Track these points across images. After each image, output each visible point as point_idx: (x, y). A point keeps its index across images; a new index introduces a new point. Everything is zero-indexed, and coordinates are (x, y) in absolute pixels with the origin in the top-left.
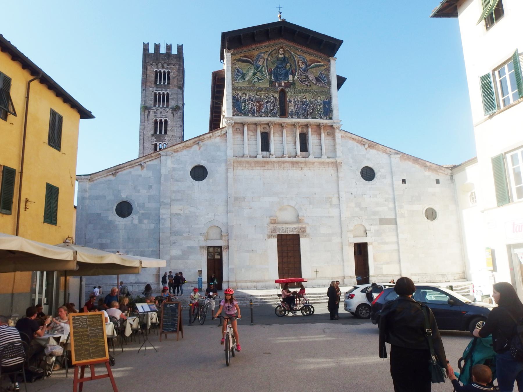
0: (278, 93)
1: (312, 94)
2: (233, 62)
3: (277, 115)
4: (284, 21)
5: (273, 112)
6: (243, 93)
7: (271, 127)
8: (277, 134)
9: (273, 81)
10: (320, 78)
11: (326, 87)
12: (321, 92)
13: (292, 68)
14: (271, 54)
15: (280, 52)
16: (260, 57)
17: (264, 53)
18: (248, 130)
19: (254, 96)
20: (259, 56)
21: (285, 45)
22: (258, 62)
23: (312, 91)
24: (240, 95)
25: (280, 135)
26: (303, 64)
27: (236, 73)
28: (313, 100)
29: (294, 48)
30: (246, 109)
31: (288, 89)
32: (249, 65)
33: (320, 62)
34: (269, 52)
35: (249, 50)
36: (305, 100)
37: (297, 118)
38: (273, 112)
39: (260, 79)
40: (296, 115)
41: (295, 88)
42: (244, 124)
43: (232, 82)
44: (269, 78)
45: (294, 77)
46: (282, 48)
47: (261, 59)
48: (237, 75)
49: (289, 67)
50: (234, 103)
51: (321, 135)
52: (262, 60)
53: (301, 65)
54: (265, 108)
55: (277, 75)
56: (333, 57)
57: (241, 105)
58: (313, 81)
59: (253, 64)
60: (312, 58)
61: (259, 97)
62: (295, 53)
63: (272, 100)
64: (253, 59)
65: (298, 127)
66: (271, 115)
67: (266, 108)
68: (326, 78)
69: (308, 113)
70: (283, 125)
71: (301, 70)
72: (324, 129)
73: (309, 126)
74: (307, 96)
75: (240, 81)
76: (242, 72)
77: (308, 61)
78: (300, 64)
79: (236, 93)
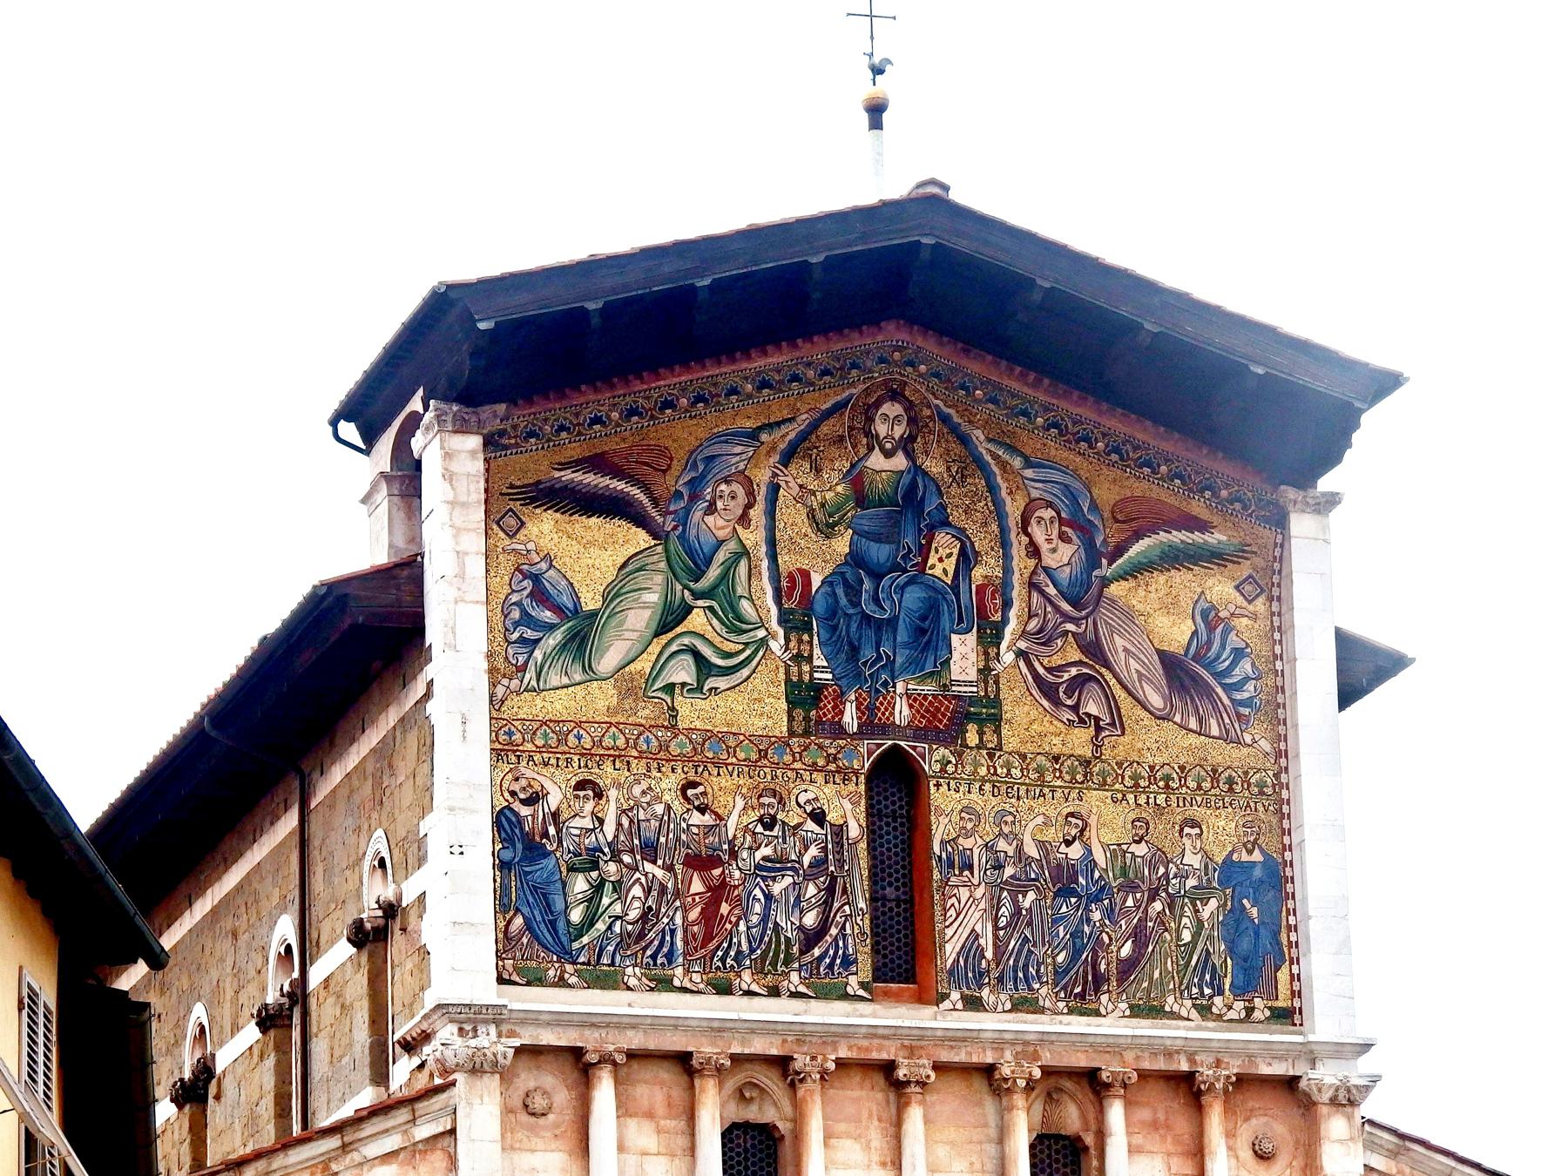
0: (862, 787)
1: (1131, 797)
2: (502, 505)
3: (853, 980)
4: (934, 197)
6: (581, 785)
7: (812, 1092)
8: (847, 1143)
10: (1197, 658)
11: (1248, 738)
12: (1206, 785)
13: (978, 573)
14: (807, 444)
15: (881, 429)
16: (718, 470)
18: (624, 1108)
19: (669, 808)
20: (712, 458)
21: (923, 368)
22: (697, 515)
23: (1136, 777)
24: (554, 800)
25: (876, 1158)
26: (1063, 538)
27: (519, 604)
28: (1140, 850)
29: (994, 401)
30: (601, 926)
31: (936, 757)
33: (1204, 527)
34: (791, 432)
35: (633, 412)
36: (1075, 852)
37: (1015, 1008)
38: (817, 952)
39: (720, 662)
41: (999, 747)
42: (592, 1058)
43: (493, 684)
44: (787, 656)
46: (895, 395)
47: (723, 487)
48: (527, 620)
49: (950, 565)
50: (503, 866)
51: (1203, 1156)
52: (730, 497)
53: (1044, 547)
54: (755, 919)
55: (854, 626)
56: (1311, 492)
57: (559, 885)
59: (655, 536)
60: (1139, 488)
61: (708, 819)
62: (1001, 444)
63: (813, 851)
65: (1019, 1100)
66: (803, 980)
67: (765, 918)
68: (1246, 667)
69: (1103, 967)
70: (901, 1073)
71: (1051, 590)
72: (1228, 1111)
73: (1108, 1086)
74: (1093, 821)
75: (555, 679)
76: (566, 601)
77: (1107, 515)
78: (1038, 533)
79: (523, 782)
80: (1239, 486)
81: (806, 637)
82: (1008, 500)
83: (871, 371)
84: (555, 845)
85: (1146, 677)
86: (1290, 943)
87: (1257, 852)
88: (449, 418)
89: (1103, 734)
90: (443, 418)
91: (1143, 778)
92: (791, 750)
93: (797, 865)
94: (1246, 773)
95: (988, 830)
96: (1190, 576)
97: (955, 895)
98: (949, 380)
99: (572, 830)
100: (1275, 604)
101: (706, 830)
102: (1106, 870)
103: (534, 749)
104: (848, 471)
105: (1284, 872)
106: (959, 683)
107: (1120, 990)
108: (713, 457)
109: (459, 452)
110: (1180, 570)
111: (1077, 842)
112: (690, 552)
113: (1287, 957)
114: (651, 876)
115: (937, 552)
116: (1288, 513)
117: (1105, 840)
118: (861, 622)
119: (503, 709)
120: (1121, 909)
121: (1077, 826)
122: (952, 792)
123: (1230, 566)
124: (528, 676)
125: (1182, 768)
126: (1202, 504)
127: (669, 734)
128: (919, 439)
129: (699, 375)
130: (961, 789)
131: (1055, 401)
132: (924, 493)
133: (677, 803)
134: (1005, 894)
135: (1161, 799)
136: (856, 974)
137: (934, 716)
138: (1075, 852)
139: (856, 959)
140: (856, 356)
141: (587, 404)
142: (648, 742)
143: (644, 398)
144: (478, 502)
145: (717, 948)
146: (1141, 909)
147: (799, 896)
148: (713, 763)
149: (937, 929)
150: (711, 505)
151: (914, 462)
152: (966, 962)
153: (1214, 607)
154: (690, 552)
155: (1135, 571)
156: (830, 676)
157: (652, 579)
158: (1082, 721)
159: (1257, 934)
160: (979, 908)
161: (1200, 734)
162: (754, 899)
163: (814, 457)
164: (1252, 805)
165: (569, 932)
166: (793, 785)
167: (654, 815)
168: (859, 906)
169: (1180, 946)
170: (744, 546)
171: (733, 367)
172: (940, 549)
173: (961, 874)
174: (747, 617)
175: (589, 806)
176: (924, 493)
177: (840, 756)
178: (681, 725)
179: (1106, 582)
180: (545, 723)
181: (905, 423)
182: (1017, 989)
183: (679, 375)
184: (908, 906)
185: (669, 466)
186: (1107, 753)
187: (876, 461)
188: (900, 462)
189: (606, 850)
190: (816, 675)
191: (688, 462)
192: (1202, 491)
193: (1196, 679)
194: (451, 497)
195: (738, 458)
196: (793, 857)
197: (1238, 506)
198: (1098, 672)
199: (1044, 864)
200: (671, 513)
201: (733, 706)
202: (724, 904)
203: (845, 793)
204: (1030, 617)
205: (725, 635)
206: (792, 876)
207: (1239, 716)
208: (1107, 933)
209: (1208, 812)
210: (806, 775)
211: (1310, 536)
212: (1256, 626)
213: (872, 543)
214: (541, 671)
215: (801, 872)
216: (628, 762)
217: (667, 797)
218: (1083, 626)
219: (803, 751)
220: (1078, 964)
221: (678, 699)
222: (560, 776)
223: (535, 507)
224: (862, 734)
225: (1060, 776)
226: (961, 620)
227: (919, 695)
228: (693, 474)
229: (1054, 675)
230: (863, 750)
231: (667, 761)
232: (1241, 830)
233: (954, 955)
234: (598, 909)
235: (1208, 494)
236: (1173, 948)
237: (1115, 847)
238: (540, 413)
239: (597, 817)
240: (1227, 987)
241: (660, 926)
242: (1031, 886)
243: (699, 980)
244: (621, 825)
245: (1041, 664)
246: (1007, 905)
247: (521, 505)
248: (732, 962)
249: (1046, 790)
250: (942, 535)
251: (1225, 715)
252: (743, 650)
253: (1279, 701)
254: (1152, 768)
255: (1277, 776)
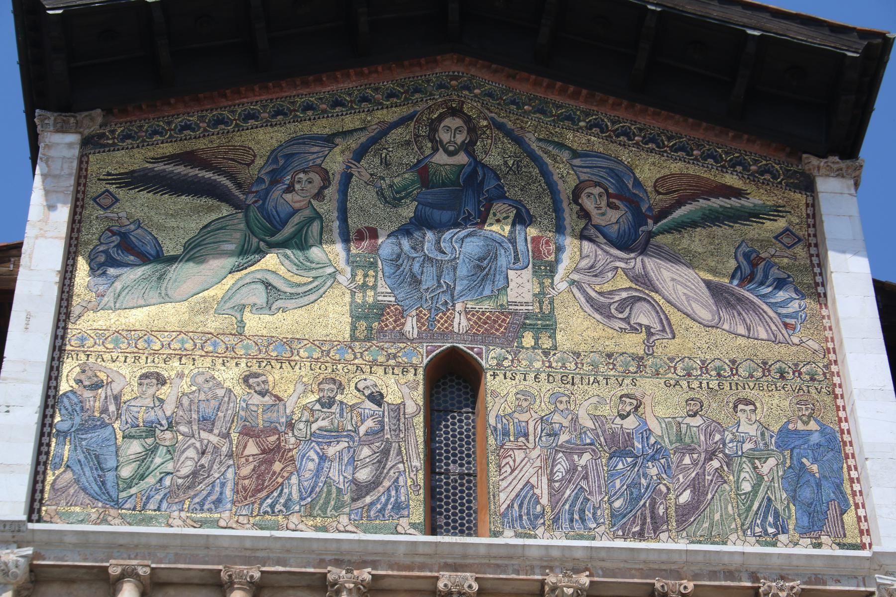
0: (420, 377)
1: (684, 384)
3: (404, 522)
5: (372, 504)
9: (389, 306)
11: (796, 340)
14: (377, 146)
15: (444, 137)
17: (329, 140)
20: (289, 157)
21: (477, 91)
26: (611, 206)
27: (105, 252)
28: (697, 421)
29: (543, 112)
30: (151, 480)
31: (492, 354)
32: (210, 209)
33: (738, 193)
34: (363, 138)
36: (631, 423)
38: (368, 499)
39: (288, 290)
40: (556, 520)
45: (547, 282)
46: (455, 112)
47: (301, 175)
52: (307, 183)
53: (594, 212)
54: (308, 475)
55: (416, 267)
57: (113, 449)
58: (694, 305)
59: (236, 205)
60: (676, 167)
63: (369, 423)
64: (241, 177)
69: (661, 511)
70: (441, 585)
74: (647, 401)
76: (150, 249)
78: (589, 204)
79: (90, 373)
80: (767, 161)
81: (371, 273)
82: (560, 182)
83: (431, 94)
84: (114, 418)
85: (696, 300)
86: (854, 494)
87: (812, 422)
88: (51, 121)
89: (655, 338)
90: (46, 122)
91: (696, 369)
92: (353, 351)
93: (352, 434)
94: (796, 365)
95: (543, 407)
96: (731, 231)
97: (510, 456)
98: (501, 98)
99: (132, 408)
100: (813, 250)
101: (265, 408)
102: (662, 437)
103: (105, 350)
104: (415, 165)
105: (842, 438)
106: (515, 303)
107: (680, 529)
108: (292, 155)
109: (58, 144)
110: (721, 227)
111: (632, 415)
112: (268, 218)
113: (851, 502)
114: (205, 442)
115: (495, 215)
116: (814, 179)
117: (661, 414)
118: (424, 261)
119: (78, 322)
120: (677, 467)
121: (631, 404)
122: (509, 380)
123: (768, 223)
124: (106, 299)
125: (733, 362)
126: (735, 177)
127: (236, 339)
128: (478, 143)
129: (277, 95)
130: (517, 377)
131: (595, 108)
132: (484, 178)
133: (238, 388)
134: (561, 455)
135: (714, 384)
136: (408, 516)
137: (492, 327)
138: (631, 423)
139: (408, 506)
140: (418, 83)
141: (178, 115)
142: (215, 345)
143: (229, 112)
144: (70, 174)
145: (267, 497)
146: (699, 466)
147: (353, 457)
148: (277, 360)
149: (491, 482)
150: (287, 188)
151: (475, 158)
152: (521, 506)
153: (755, 251)
154: (268, 218)
155: (680, 227)
156: (393, 299)
157: (231, 235)
158: (634, 329)
159: (819, 485)
160: (535, 465)
161: (748, 337)
162: (307, 459)
163: (383, 155)
164: (805, 388)
165: (118, 485)
166: (353, 375)
167: (215, 397)
168: (414, 464)
169: (740, 495)
170: (317, 213)
171: (308, 90)
172: (498, 214)
173: (516, 440)
174: (316, 260)
175: (151, 391)
176: (484, 178)
177: (400, 354)
178: (247, 333)
179: (652, 235)
180: (118, 332)
181: (466, 132)
182: (572, 528)
183: (260, 95)
184: (472, 478)
185: (253, 161)
186: (658, 351)
187: (441, 158)
188: (462, 158)
189: (164, 422)
190: (380, 298)
191: (269, 157)
192: (734, 166)
193: (740, 300)
194: (46, 170)
195: (315, 156)
196: (350, 428)
197: (768, 176)
198: (648, 295)
199: (600, 434)
200: (253, 192)
201: (299, 319)
202: (277, 463)
203: (402, 381)
204: (582, 258)
205: (297, 272)
206: (348, 442)
207: (786, 325)
208: (665, 485)
209: (761, 393)
210: (367, 369)
211: (837, 191)
212: (797, 263)
213: (435, 210)
214: (119, 296)
215: (357, 439)
216: (194, 360)
217: (228, 384)
218: (632, 264)
219: (364, 351)
220: (637, 508)
221: (247, 315)
222: (125, 370)
223: (129, 189)
224: (420, 338)
225: (613, 368)
226: (517, 259)
227: (477, 312)
228: (275, 167)
229: (605, 297)
230: (423, 351)
231: (232, 358)
232: (796, 407)
233: (508, 502)
234: (149, 467)
235: (739, 168)
236: (733, 496)
237: (670, 419)
238: (135, 121)
239: (158, 398)
240: (791, 527)
241: (211, 479)
242: (587, 449)
243: (245, 522)
244: (181, 404)
245: (594, 289)
246: (563, 463)
247: (116, 187)
248: (282, 508)
249: (600, 378)
250: (500, 205)
251: (772, 325)
252: (311, 282)
253: (824, 314)
254: (703, 362)
255: (827, 367)
